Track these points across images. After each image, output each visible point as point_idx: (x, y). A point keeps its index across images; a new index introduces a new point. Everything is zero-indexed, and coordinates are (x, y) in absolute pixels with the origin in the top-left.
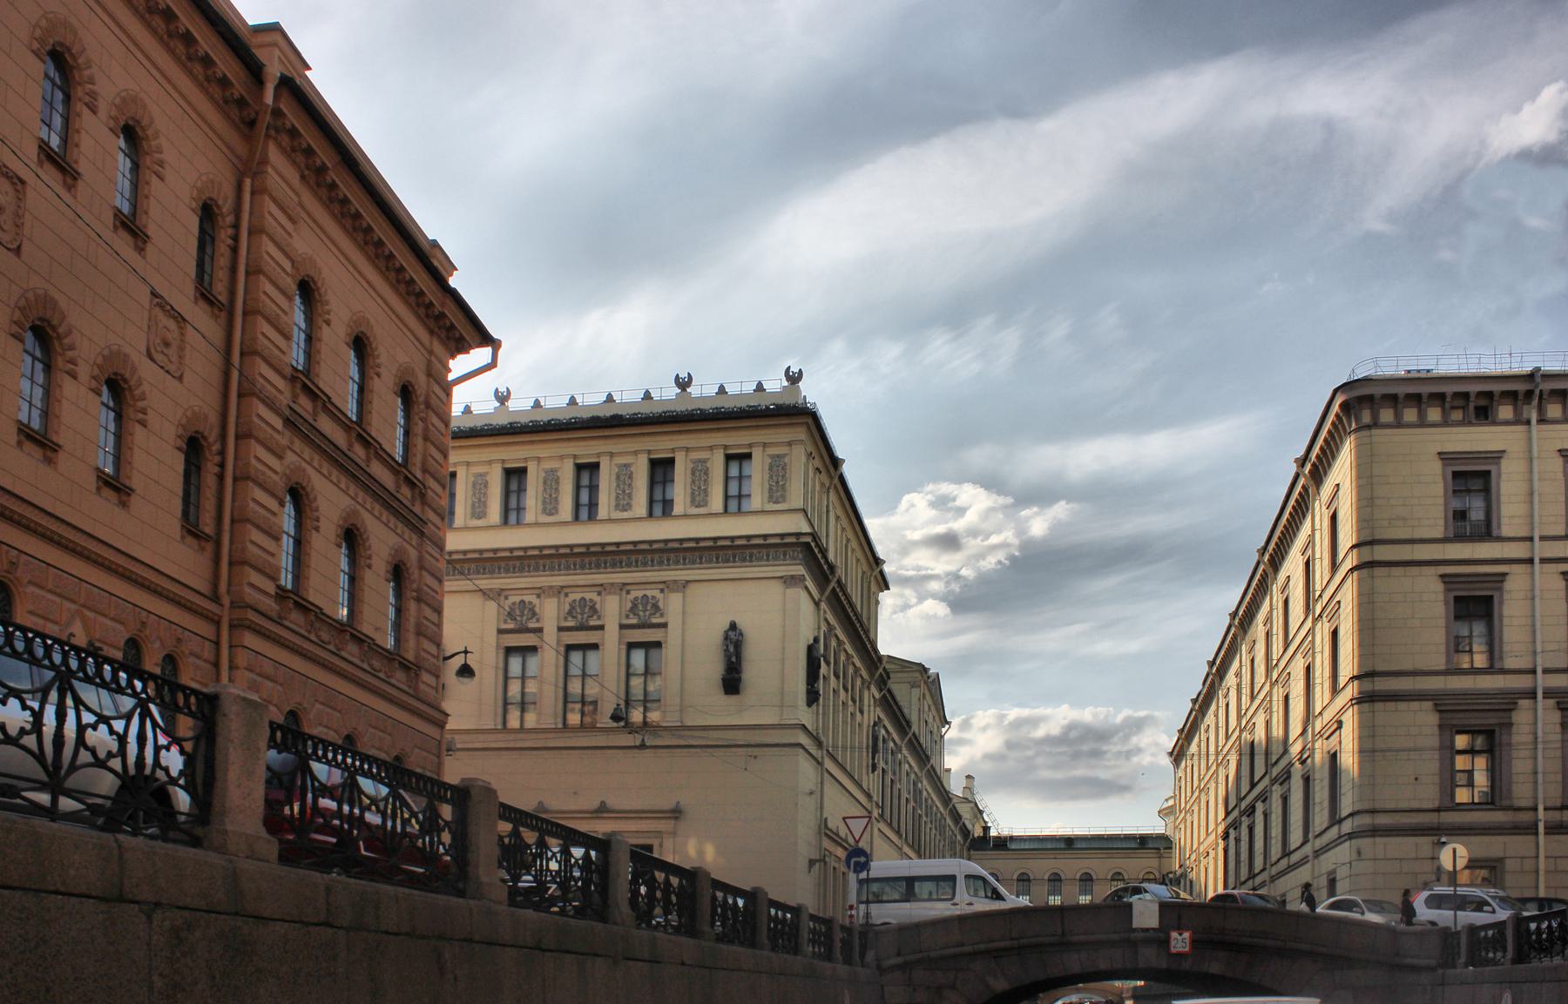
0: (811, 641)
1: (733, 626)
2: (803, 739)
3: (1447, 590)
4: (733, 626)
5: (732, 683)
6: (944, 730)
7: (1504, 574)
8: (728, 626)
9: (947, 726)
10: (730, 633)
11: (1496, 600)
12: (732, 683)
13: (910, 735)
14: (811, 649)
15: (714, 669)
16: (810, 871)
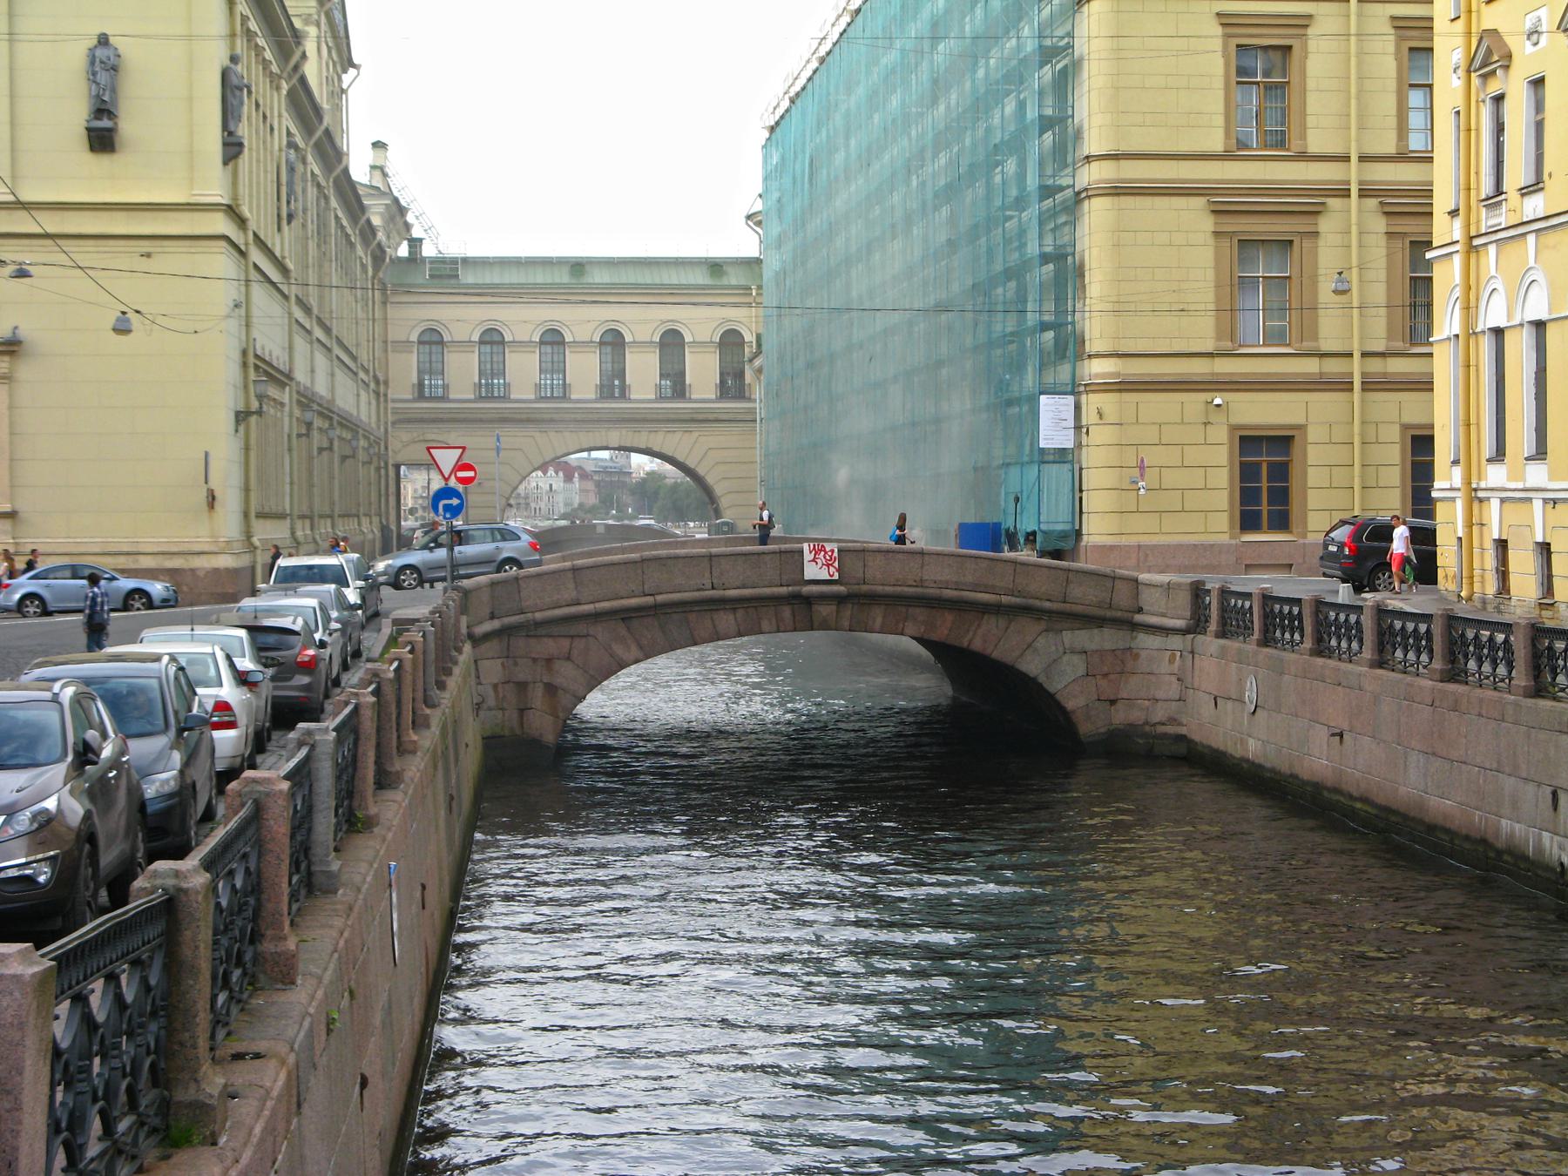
0: (227, 62)
1: (103, 40)
2: (220, 224)
3: (1227, 36)
4: (103, 40)
5: (102, 140)
6: (347, 78)
7: (1310, 16)
8: (95, 42)
9: (352, 72)
10: (99, 53)
11: (1296, 51)
12: (102, 140)
13: (319, 133)
14: (225, 75)
15: (77, 114)
16: (237, 431)
